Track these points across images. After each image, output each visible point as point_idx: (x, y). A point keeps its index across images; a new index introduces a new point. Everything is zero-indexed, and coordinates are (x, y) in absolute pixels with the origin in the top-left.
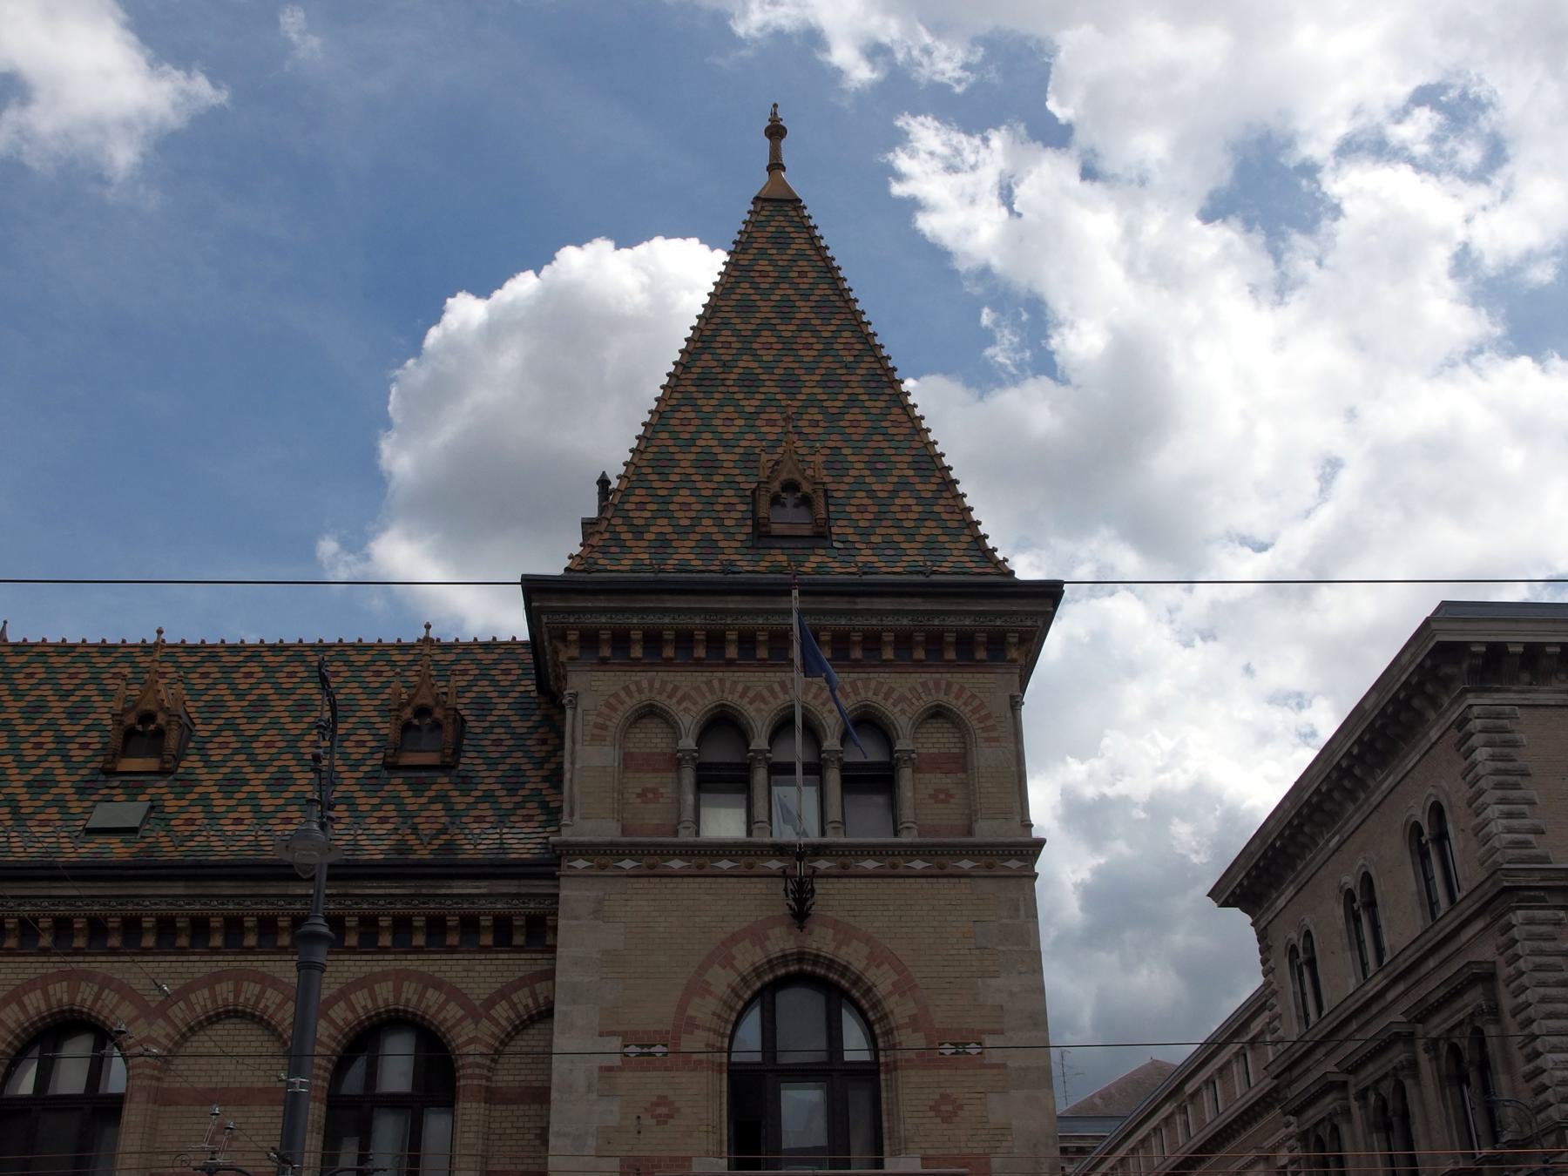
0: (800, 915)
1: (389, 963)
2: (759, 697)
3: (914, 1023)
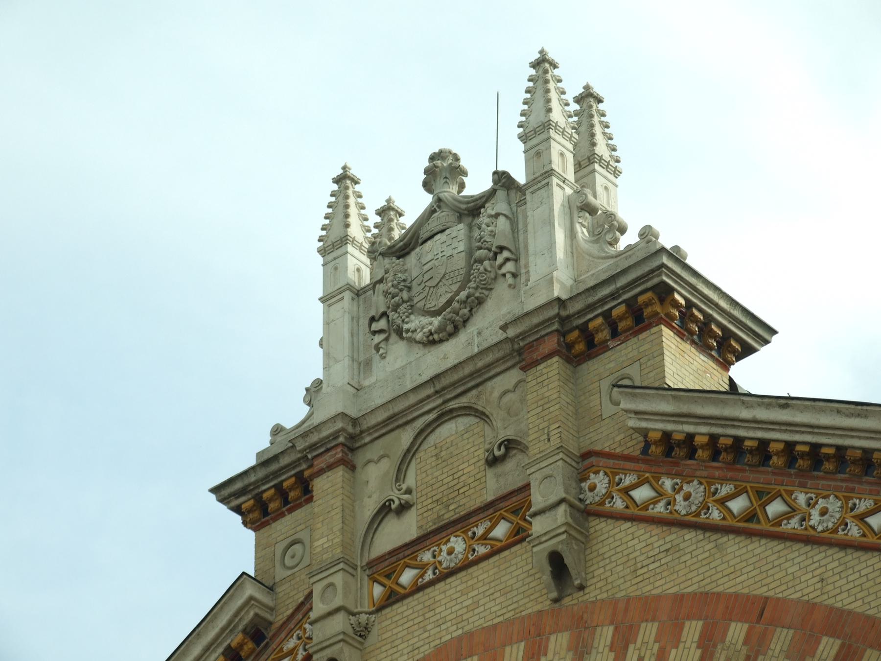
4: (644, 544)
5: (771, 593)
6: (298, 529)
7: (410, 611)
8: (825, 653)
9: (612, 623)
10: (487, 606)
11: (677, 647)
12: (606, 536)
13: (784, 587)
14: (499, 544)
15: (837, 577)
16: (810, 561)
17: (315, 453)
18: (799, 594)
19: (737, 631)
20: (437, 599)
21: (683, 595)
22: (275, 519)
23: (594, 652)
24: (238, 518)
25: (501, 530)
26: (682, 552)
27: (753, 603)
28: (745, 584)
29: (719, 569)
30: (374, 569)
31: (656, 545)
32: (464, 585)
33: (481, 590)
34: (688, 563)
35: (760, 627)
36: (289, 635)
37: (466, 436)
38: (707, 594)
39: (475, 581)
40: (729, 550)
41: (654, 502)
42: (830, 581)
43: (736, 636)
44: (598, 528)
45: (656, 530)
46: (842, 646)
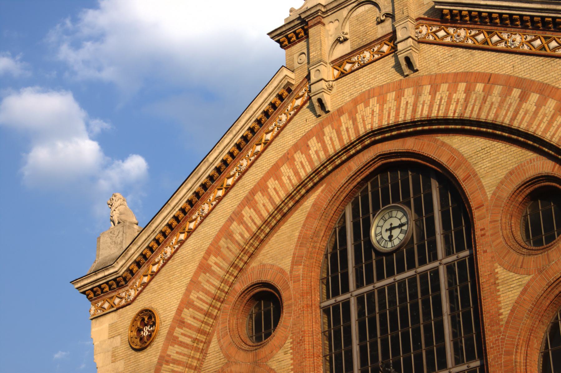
4: (442, 53)
5: (493, 72)
6: (303, 48)
7: (349, 80)
8: (515, 95)
9: (430, 84)
10: (380, 78)
11: (455, 93)
12: (427, 50)
13: (498, 70)
14: (384, 54)
15: (520, 65)
16: (508, 59)
17: (309, 19)
18: (504, 72)
19: (479, 87)
20: (360, 75)
21: (458, 73)
22: (293, 45)
23: (423, 95)
24: (278, 45)
25: (385, 48)
26: (457, 57)
27: (486, 76)
28: (483, 68)
29: (472, 63)
30: (334, 64)
31: (447, 54)
32: (370, 70)
33: (377, 72)
34: (460, 61)
35: (489, 85)
36: (301, 89)
37: (369, 12)
38: (467, 72)
39: (374, 68)
40: (476, 56)
41: (446, 37)
42: (517, 67)
43: (479, 88)
44: (423, 47)
45: (447, 48)
46: (522, 92)
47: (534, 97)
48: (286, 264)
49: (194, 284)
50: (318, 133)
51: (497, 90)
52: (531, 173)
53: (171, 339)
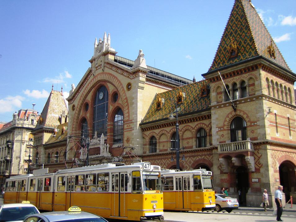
0: (235, 110)
1: (199, 122)
2: (230, 82)
3: (249, 121)
47: (115, 79)
48: (89, 100)
49: (79, 101)
50: (93, 79)
51: (112, 76)
52: (114, 91)
53: (77, 110)
